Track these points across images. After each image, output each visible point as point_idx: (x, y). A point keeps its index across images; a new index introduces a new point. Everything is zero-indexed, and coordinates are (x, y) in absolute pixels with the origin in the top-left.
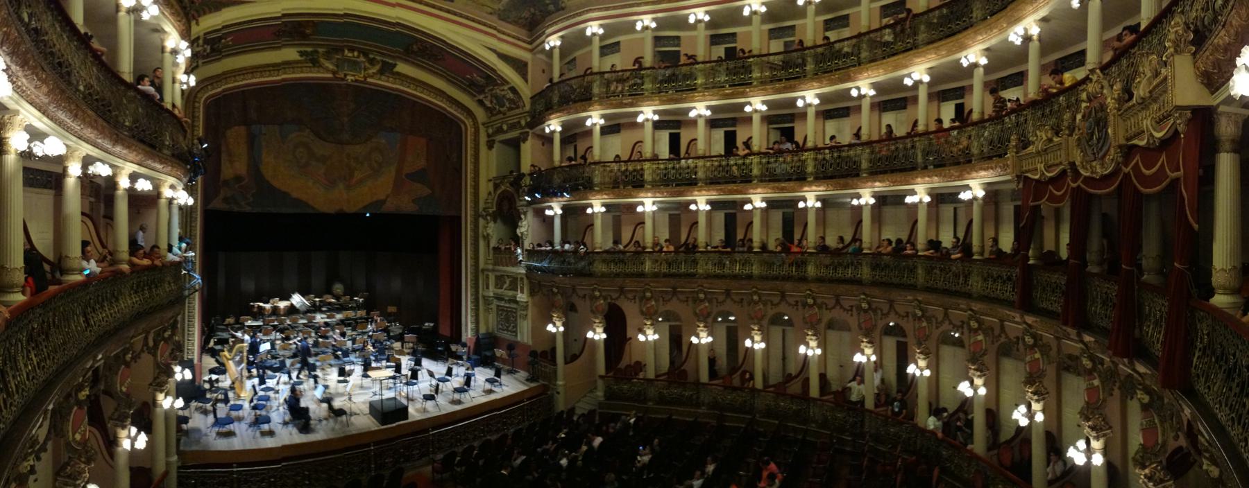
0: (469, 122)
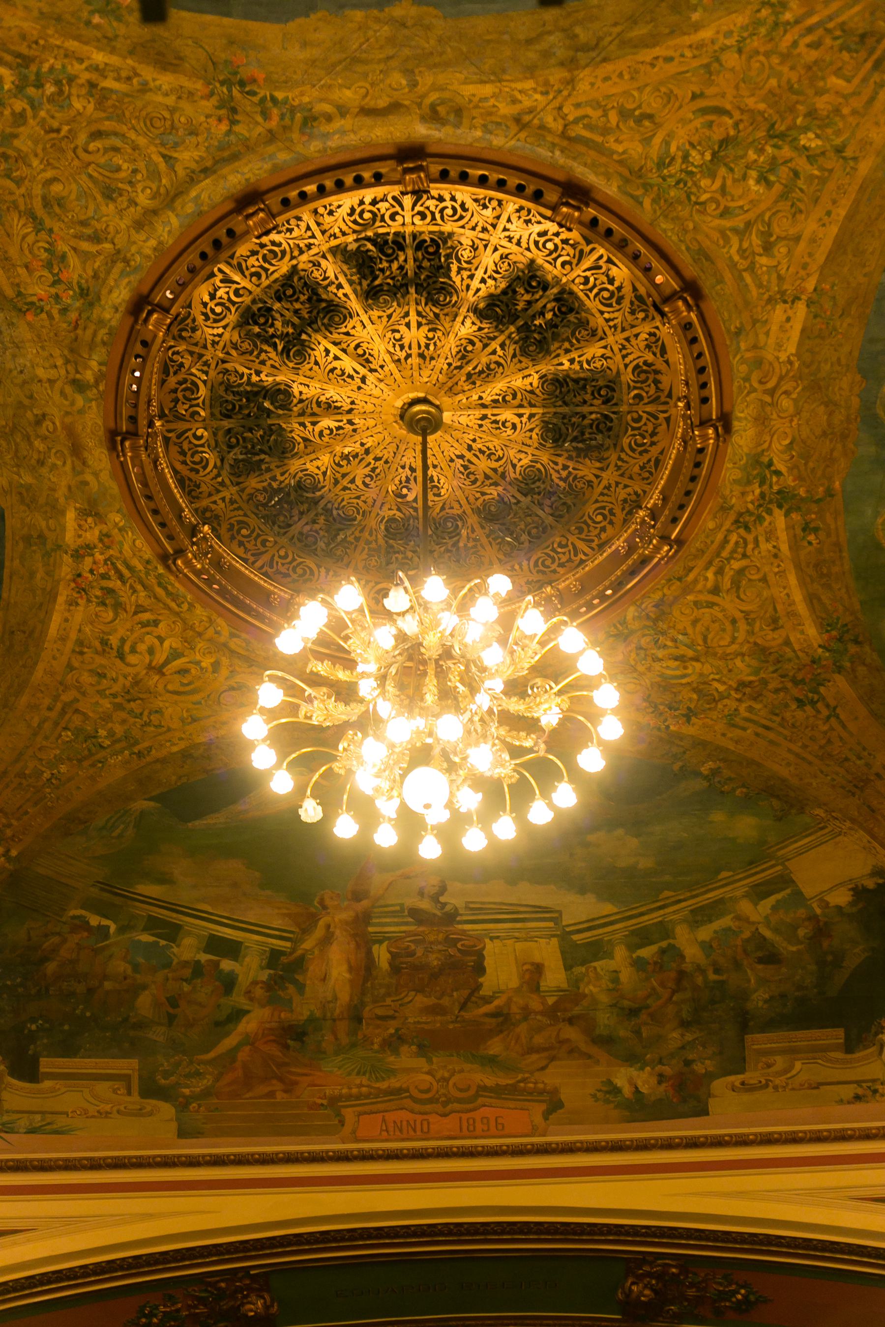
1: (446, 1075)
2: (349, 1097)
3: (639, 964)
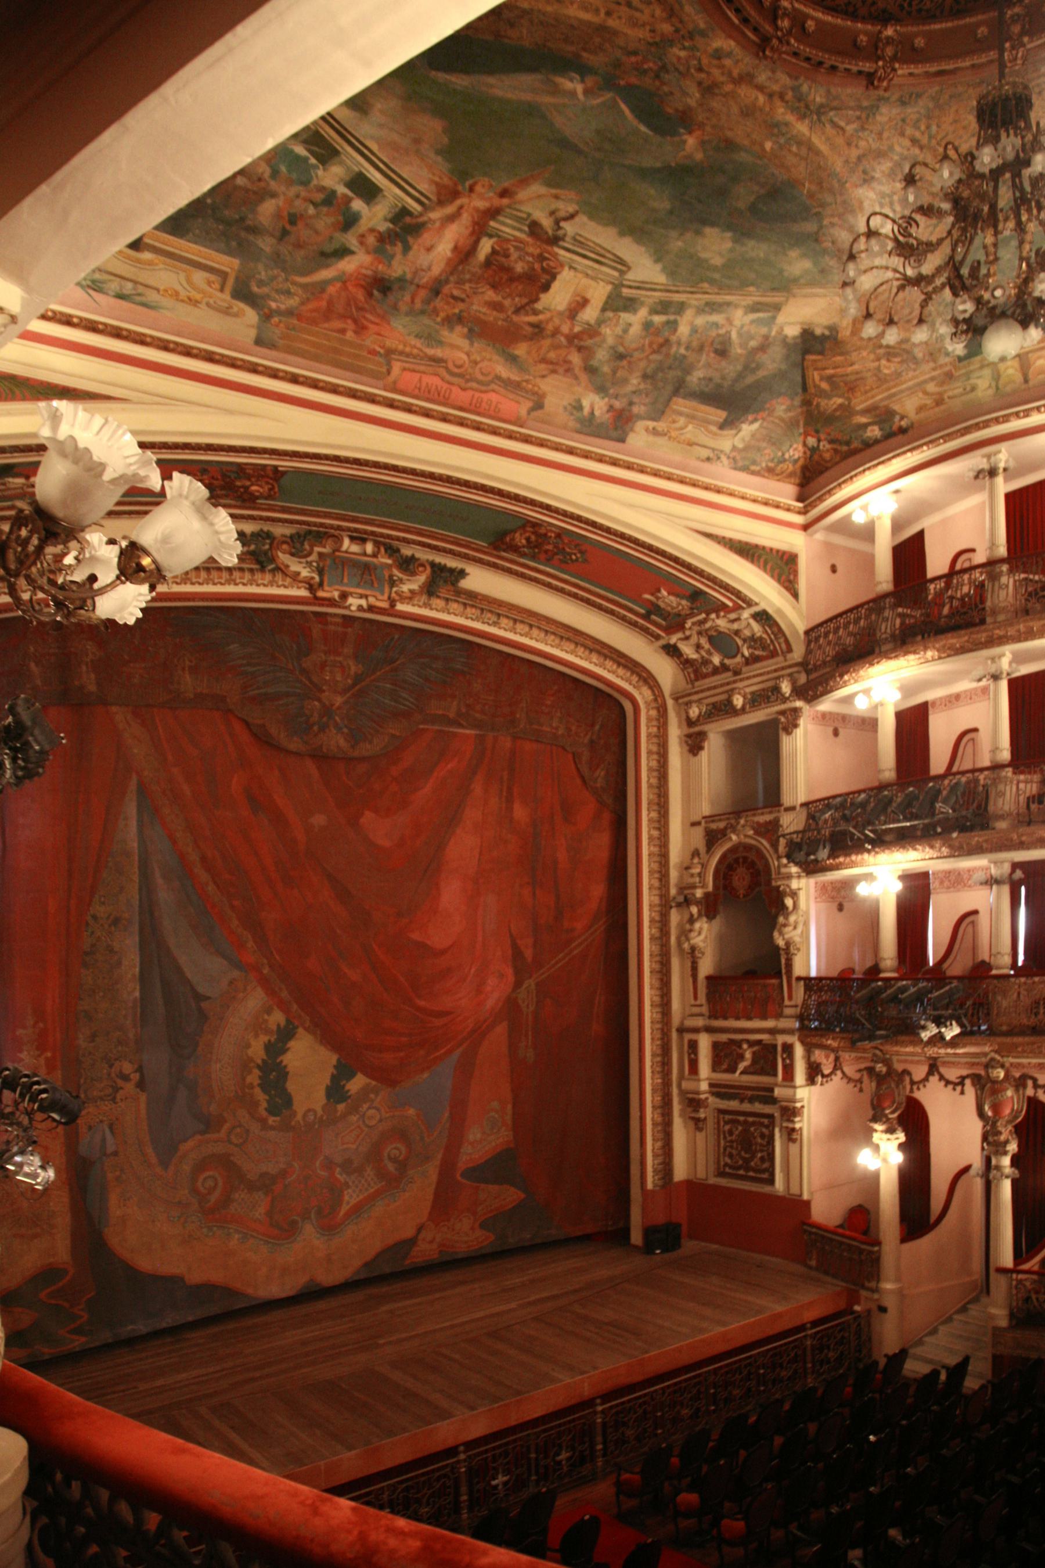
0: (643, 696)
1: (478, 359)
2: (401, 353)
3: (647, 325)
